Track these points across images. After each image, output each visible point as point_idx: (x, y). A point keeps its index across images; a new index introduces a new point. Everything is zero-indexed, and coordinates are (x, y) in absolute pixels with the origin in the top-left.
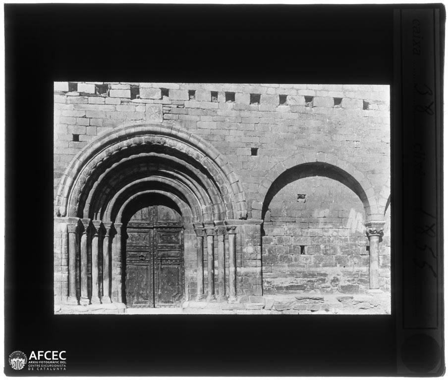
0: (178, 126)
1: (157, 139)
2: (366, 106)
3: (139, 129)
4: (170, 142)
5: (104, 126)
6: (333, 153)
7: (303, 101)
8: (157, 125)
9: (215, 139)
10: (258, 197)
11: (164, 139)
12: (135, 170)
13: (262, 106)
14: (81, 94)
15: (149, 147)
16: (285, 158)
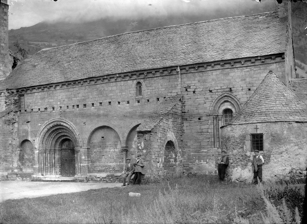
0: (64, 119)
1: (58, 123)
2: (119, 103)
3: (54, 121)
4: (62, 124)
5: (46, 120)
6: (108, 122)
7: (99, 104)
8: (58, 119)
9: (73, 121)
10: (86, 139)
11: (60, 123)
12: (58, 132)
13: (87, 108)
14: (41, 112)
15: (57, 125)
16: (93, 125)
